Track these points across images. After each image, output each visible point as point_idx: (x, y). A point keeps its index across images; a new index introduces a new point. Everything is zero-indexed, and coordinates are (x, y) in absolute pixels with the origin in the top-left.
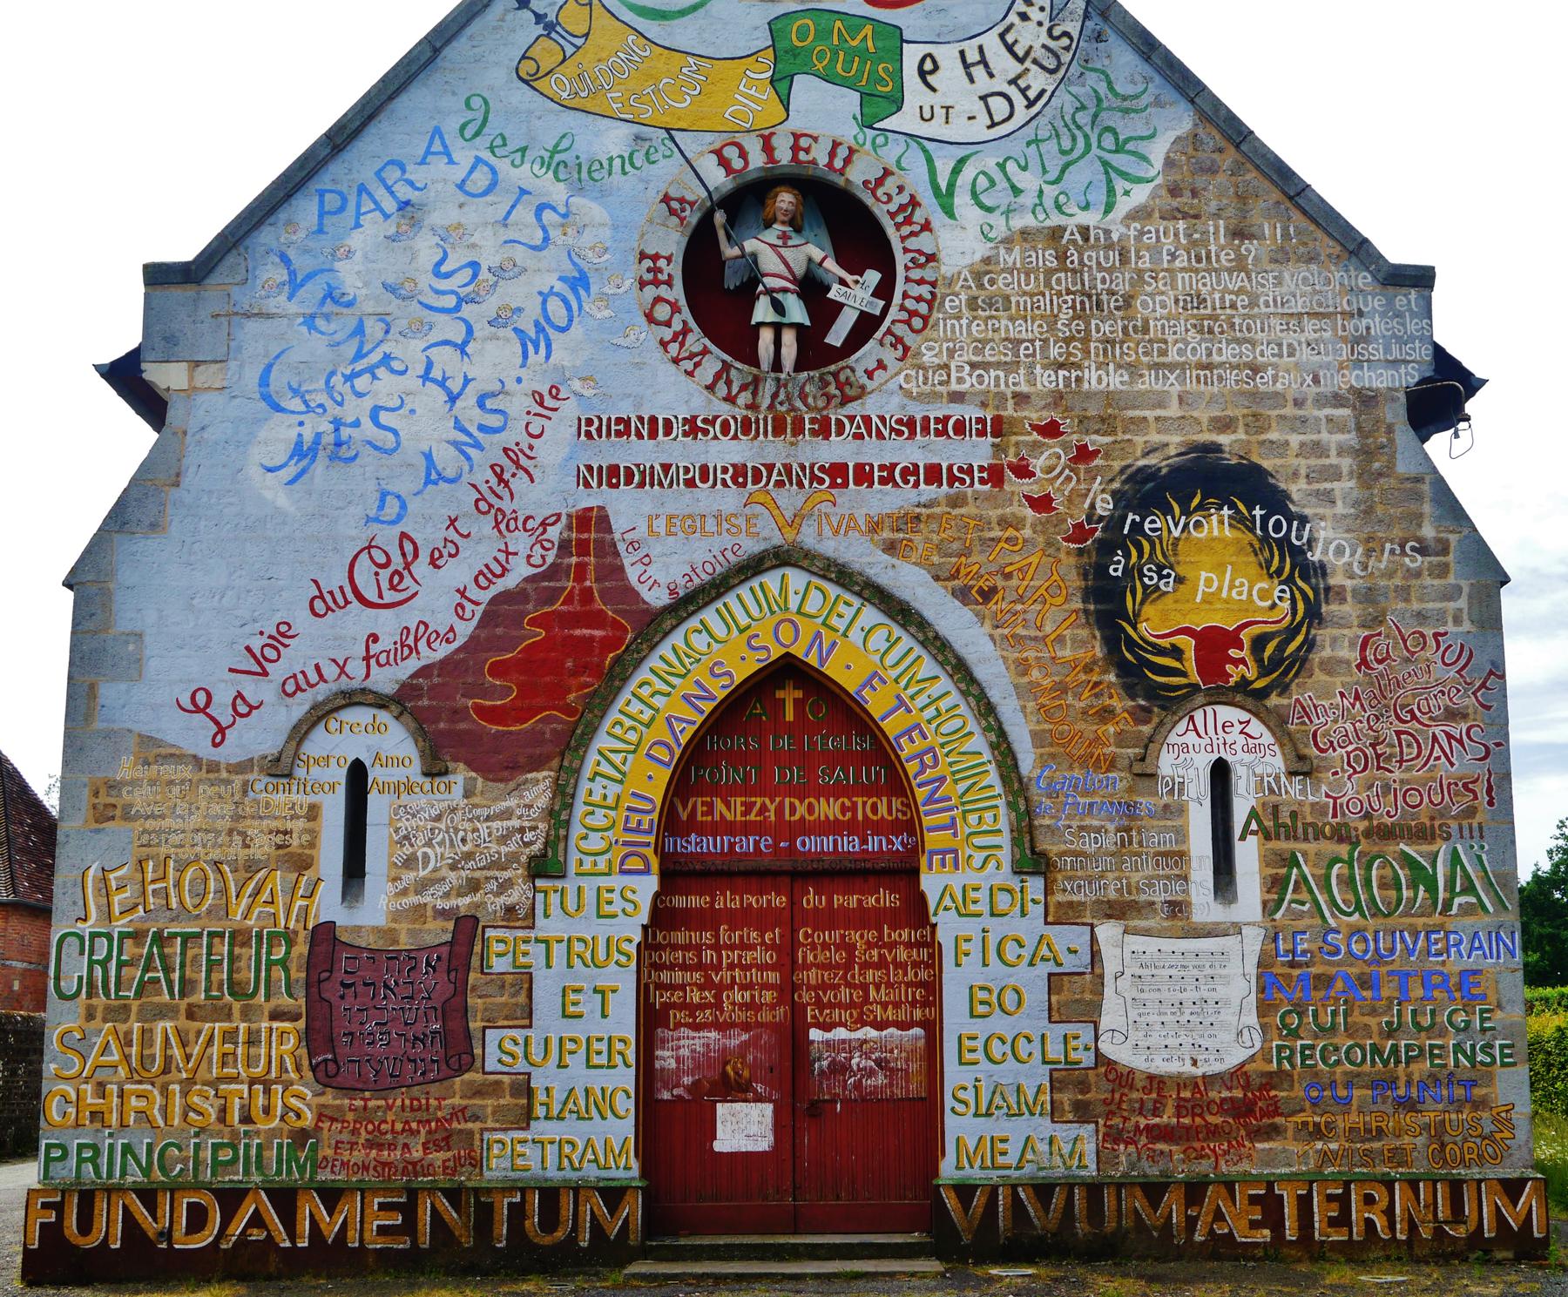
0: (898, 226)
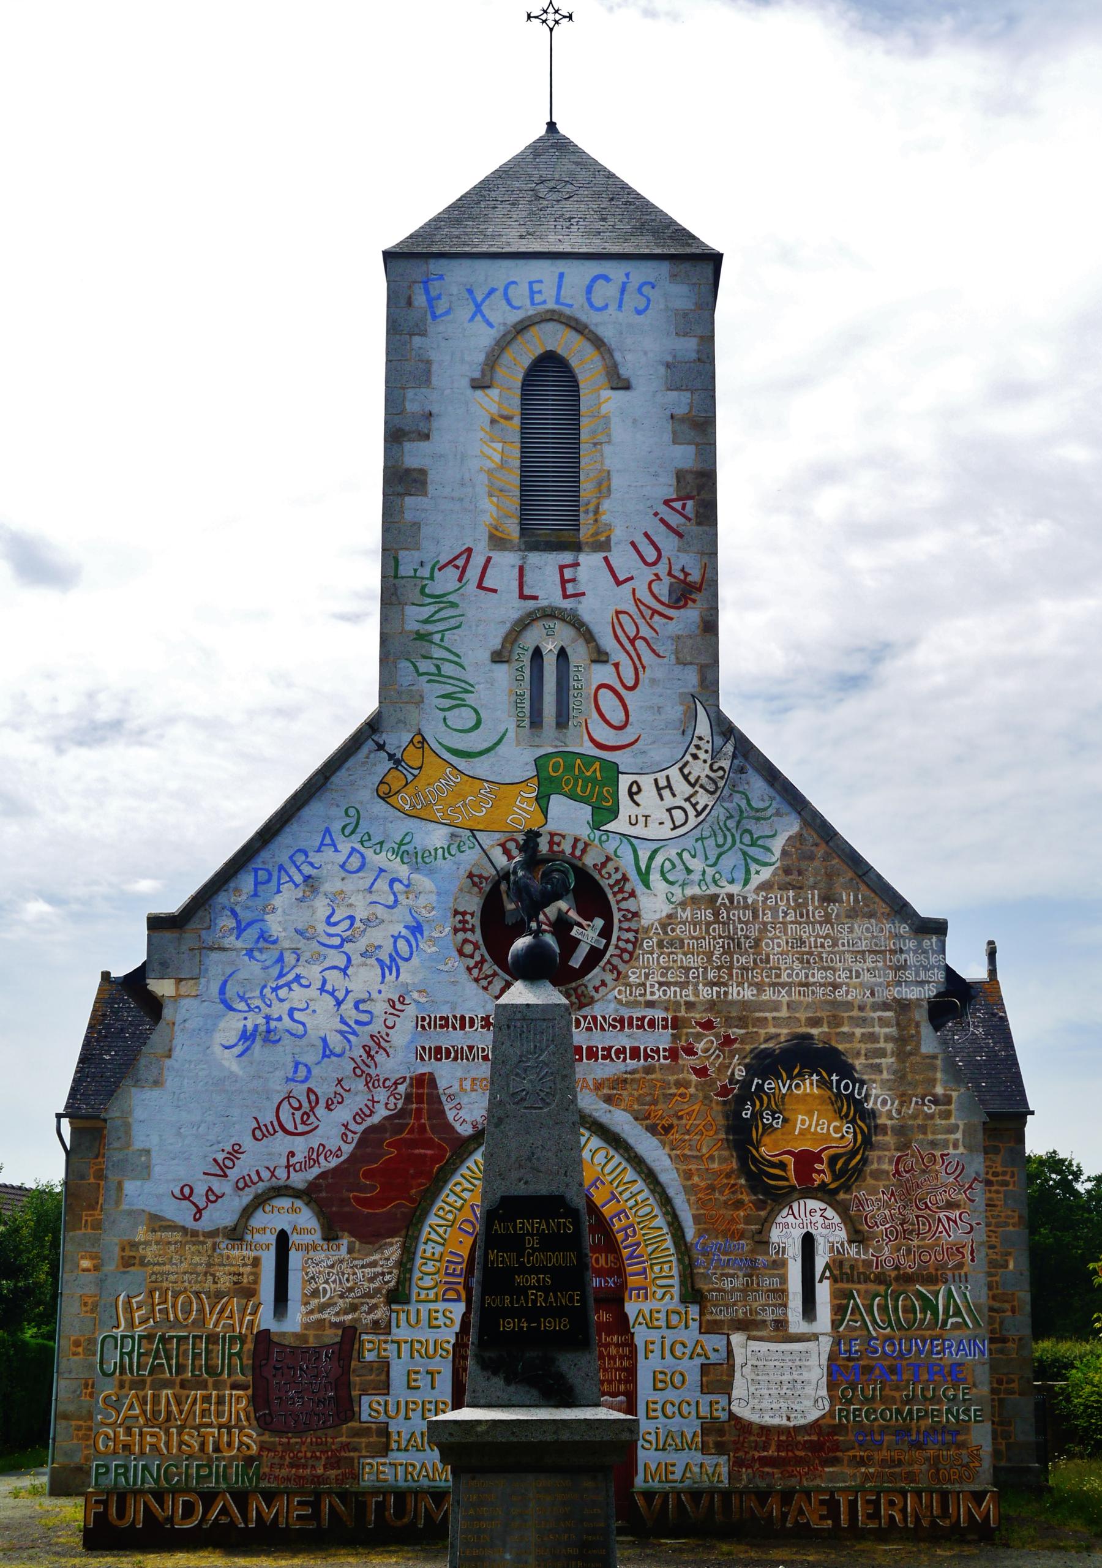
0: (615, 894)
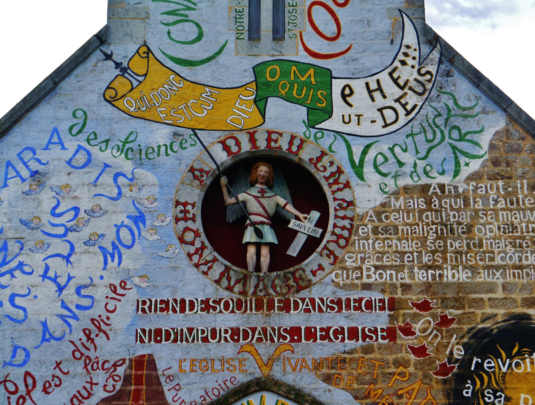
0: (330, 185)
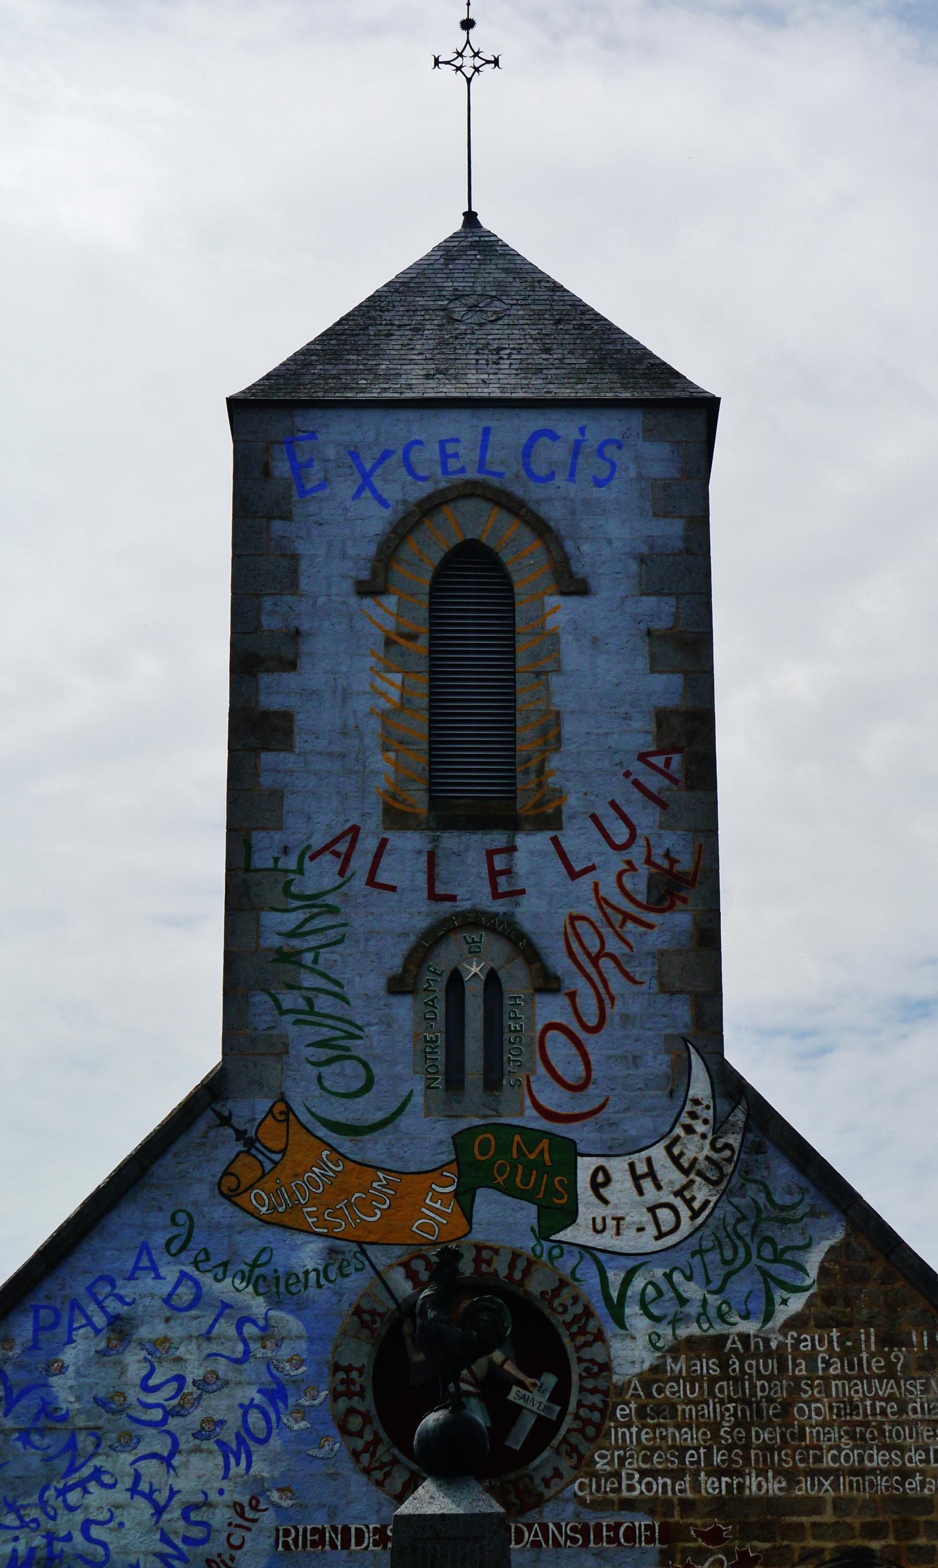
0: (573, 1337)
